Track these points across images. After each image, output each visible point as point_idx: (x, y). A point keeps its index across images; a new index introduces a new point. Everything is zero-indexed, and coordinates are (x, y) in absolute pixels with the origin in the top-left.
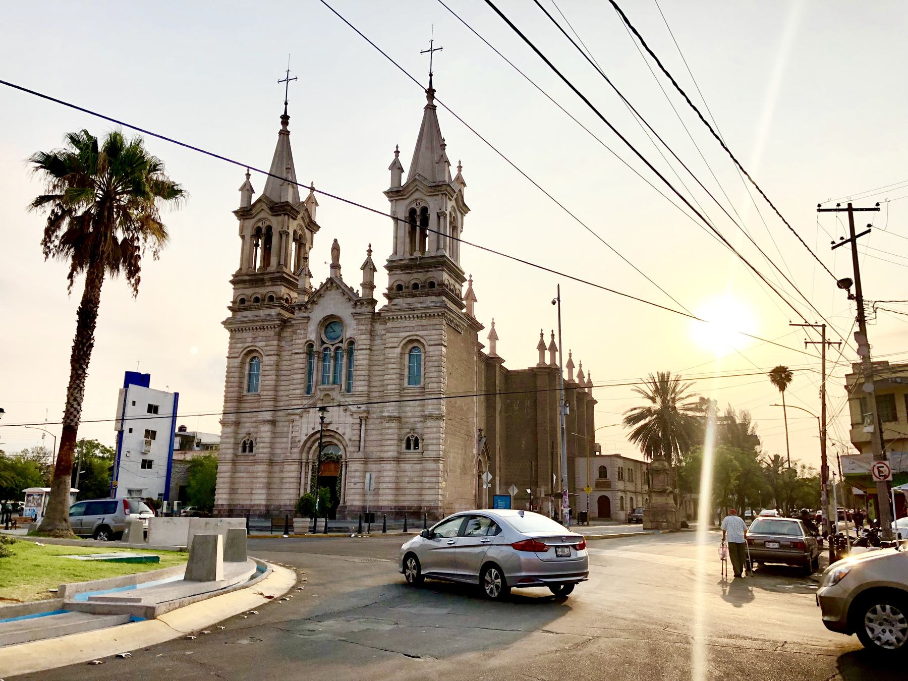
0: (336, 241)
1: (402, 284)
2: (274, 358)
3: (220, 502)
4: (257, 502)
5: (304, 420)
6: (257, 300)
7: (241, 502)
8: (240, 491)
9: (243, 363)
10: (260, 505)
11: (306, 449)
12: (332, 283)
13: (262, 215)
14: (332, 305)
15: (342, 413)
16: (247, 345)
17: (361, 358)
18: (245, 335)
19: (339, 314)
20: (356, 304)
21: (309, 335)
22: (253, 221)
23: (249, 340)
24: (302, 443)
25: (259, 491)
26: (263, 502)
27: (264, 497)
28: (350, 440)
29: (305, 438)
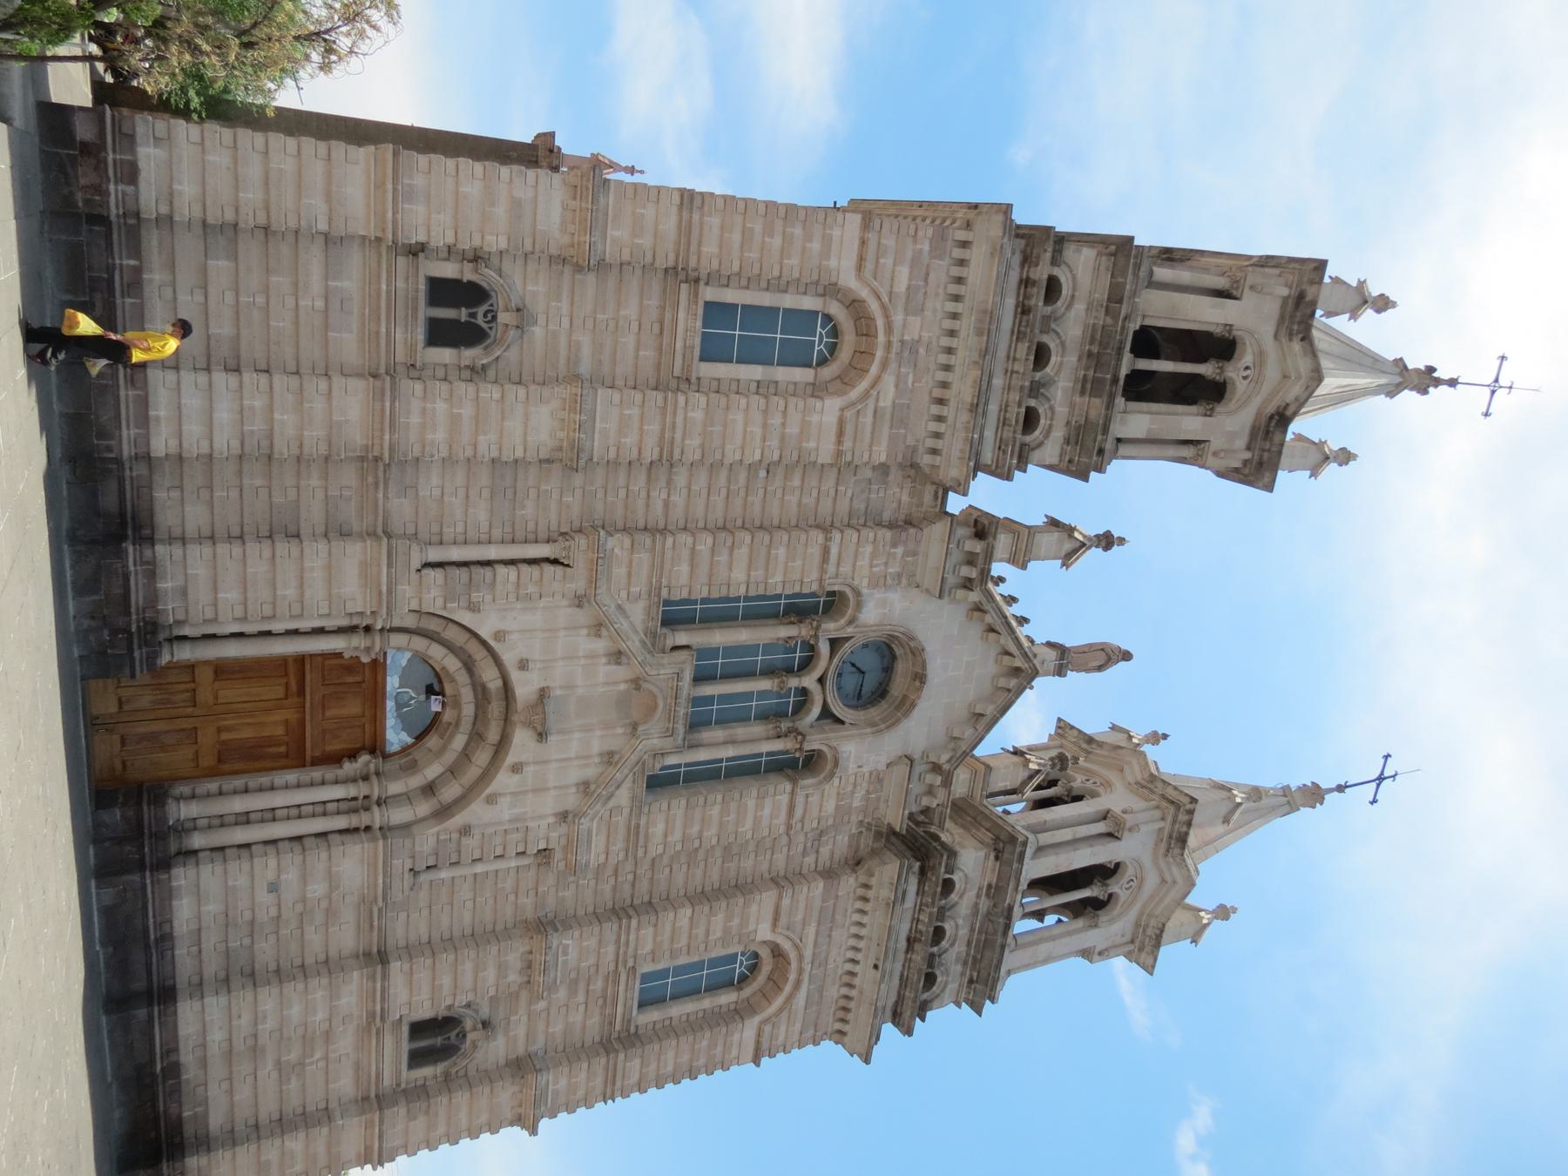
0: (1127, 656)
1: (954, 897)
2: (825, 456)
3: (148, 156)
4: (161, 408)
5: (565, 613)
6: (1041, 356)
7: (155, 276)
8: (220, 266)
9: (831, 290)
10: (144, 420)
11: (433, 625)
12: (1017, 671)
13: (1272, 373)
14: (953, 661)
15: (575, 775)
16: (898, 318)
17: (763, 809)
18: (938, 306)
19: (916, 713)
20: (936, 768)
21: (878, 595)
22: (1267, 330)
23: (915, 328)
24: (466, 618)
25: (224, 414)
26: (161, 444)
27: (194, 438)
28: (465, 831)
29: (485, 633)
